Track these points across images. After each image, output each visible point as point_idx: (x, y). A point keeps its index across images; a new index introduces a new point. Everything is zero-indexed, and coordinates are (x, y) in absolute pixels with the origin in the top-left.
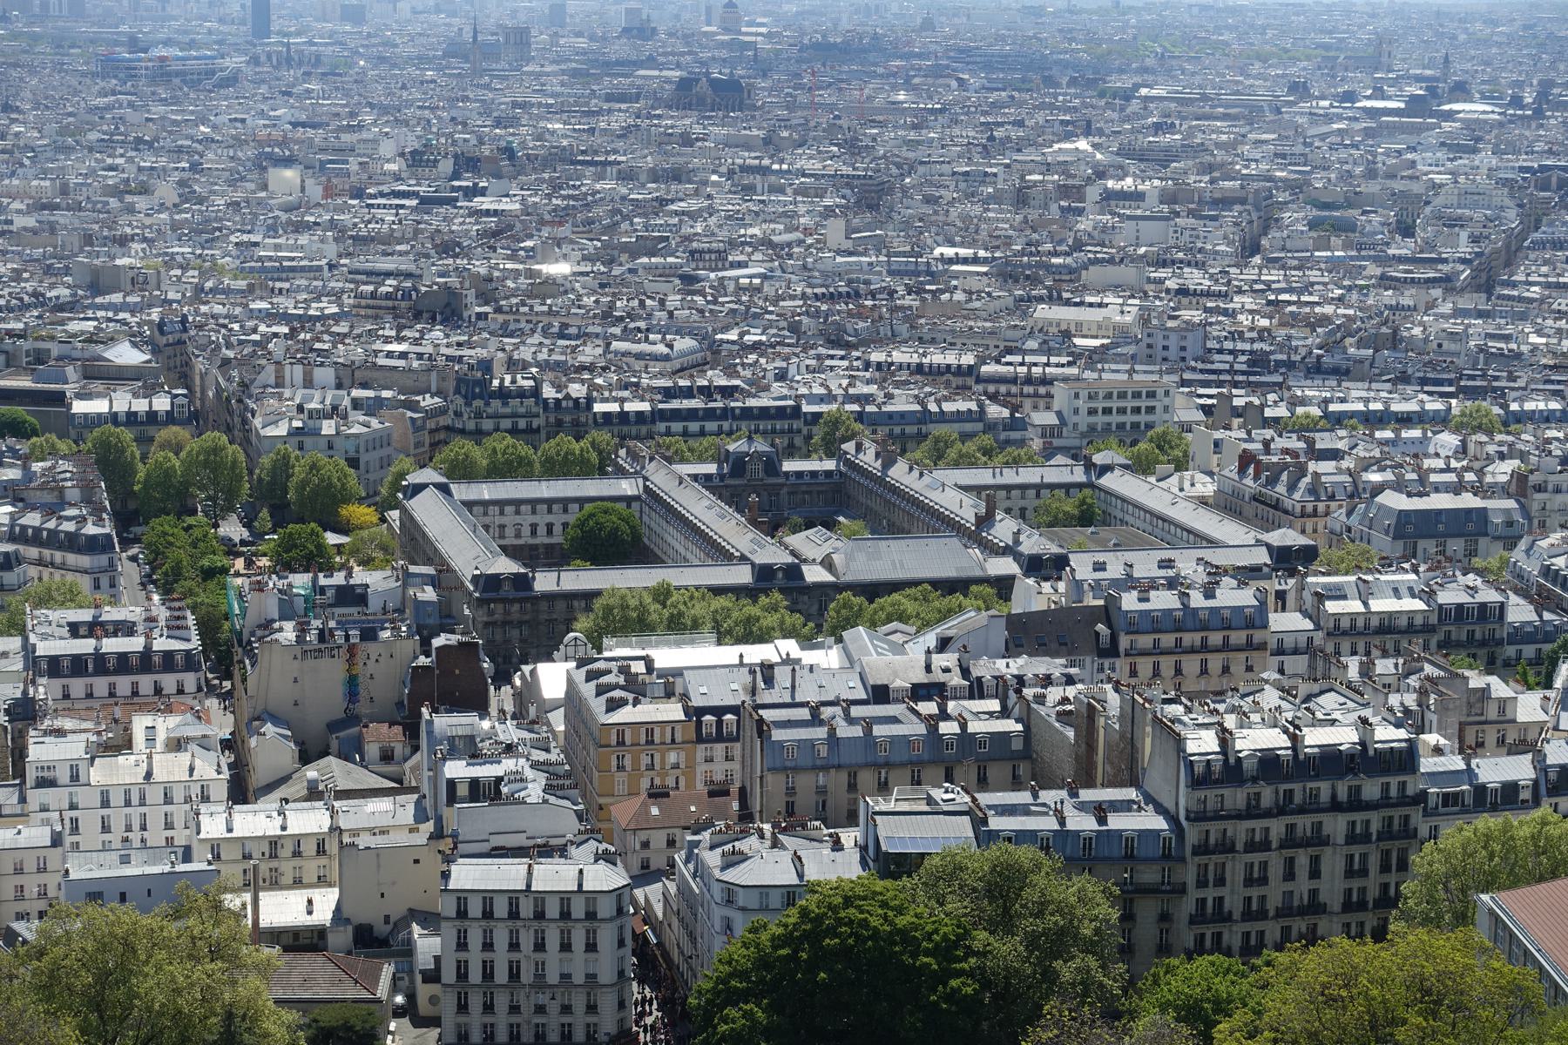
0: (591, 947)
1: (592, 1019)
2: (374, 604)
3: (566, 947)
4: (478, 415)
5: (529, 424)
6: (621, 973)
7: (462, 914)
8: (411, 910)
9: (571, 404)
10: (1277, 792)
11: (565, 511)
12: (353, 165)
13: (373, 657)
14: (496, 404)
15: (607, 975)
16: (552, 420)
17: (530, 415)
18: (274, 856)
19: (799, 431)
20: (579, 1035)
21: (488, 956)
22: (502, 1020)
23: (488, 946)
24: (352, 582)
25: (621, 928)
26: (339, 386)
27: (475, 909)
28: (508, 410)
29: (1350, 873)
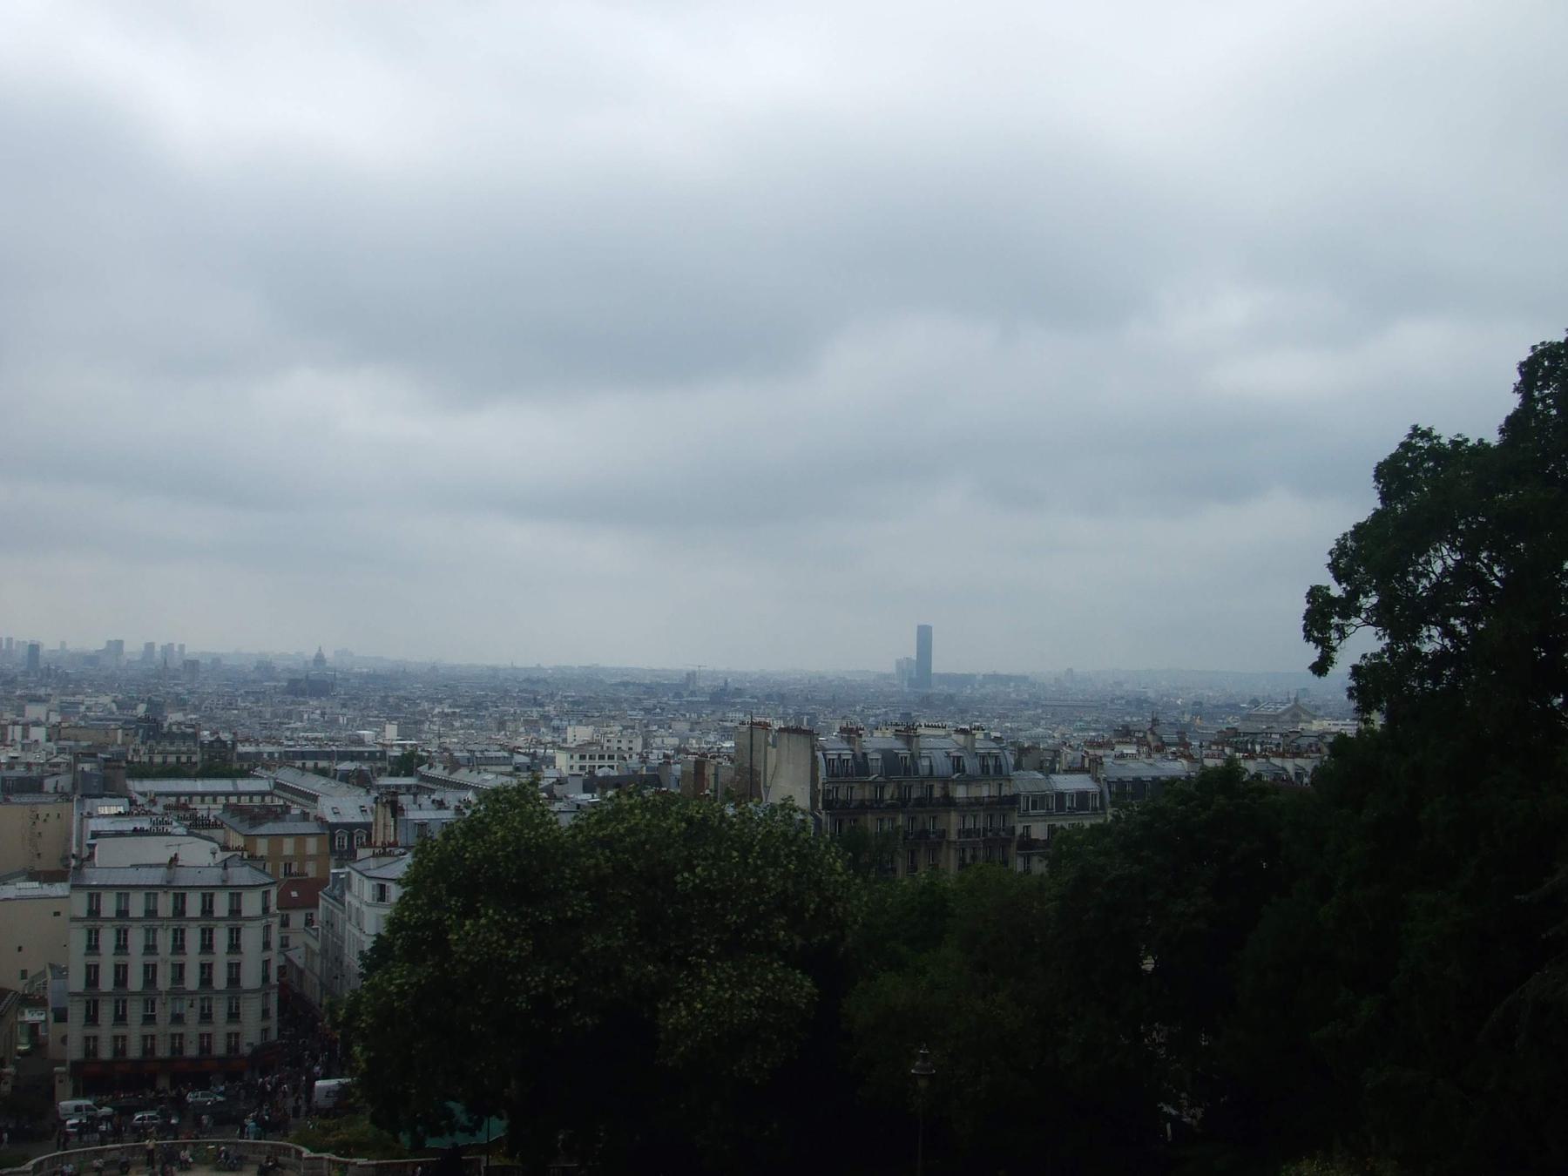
0: (234, 947)
1: (234, 1028)
2: (49, 784)
3: (207, 946)
4: (151, 751)
5: (189, 759)
6: (266, 979)
7: (94, 913)
8: (52, 966)
11: (215, 801)
12: (82, 708)
13: (42, 817)
15: (251, 977)
16: (206, 757)
17: (190, 753)
19: (385, 769)
20: (219, 1048)
21: (122, 959)
23: (122, 947)
24: (30, 774)
25: (267, 928)
26: (49, 740)
27: (109, 905)
28: (173, 749)
29: (963, 865)
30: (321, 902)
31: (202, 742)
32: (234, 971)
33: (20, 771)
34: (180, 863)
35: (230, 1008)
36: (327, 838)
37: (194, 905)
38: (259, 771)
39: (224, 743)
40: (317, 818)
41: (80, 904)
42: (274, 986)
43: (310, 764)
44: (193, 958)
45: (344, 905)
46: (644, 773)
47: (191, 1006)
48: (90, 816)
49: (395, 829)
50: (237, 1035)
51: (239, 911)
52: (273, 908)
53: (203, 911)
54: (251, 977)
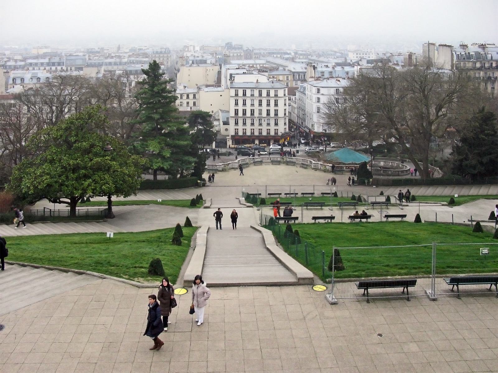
0: (276, 105)
1: (276, 128)
2: (209, 62)
3: (268, 105)
6: (285, 114)
7: (237, 95)
8: (220, 110)
9: (249, 50)
10: (481, 63)
14: (234, 51)
18: (181, 98)
20: (272, 133)
21: (244, 108)
22: (248, 128)
23: (244, 104)
25: (285, 100)
28: (236, 52)
30: (297, 93)
31: (244, 50)
32: (276, 111)
33: (200, 58)
34: (258, 82)
35: (275, 122)
36: (292, 76)
37: (264, 93)
38: (261, 58)
39: (250, 50)
40: (288, 70)
41: (233, 92)
42: (287, 116)
43: (275, 56)
44: (264, 108)
45: (305, 94)
46: (385, 58)
47: (264, 121)
48: (229, 69)
49: (315, 73)
50: (277, 130)
51: (277, 95)
52: (287, 95)
53: (267, 95)
54: (281, 114)
